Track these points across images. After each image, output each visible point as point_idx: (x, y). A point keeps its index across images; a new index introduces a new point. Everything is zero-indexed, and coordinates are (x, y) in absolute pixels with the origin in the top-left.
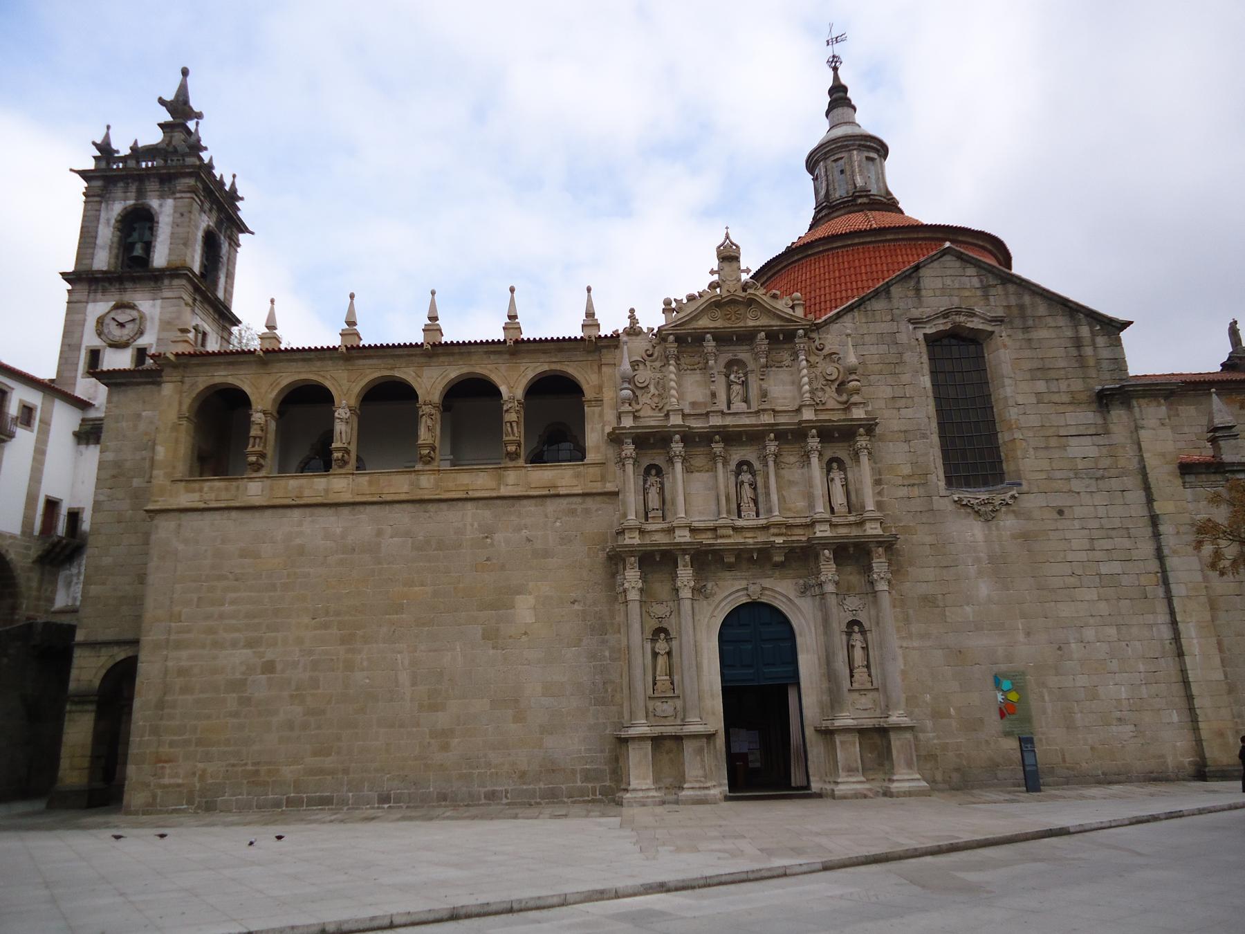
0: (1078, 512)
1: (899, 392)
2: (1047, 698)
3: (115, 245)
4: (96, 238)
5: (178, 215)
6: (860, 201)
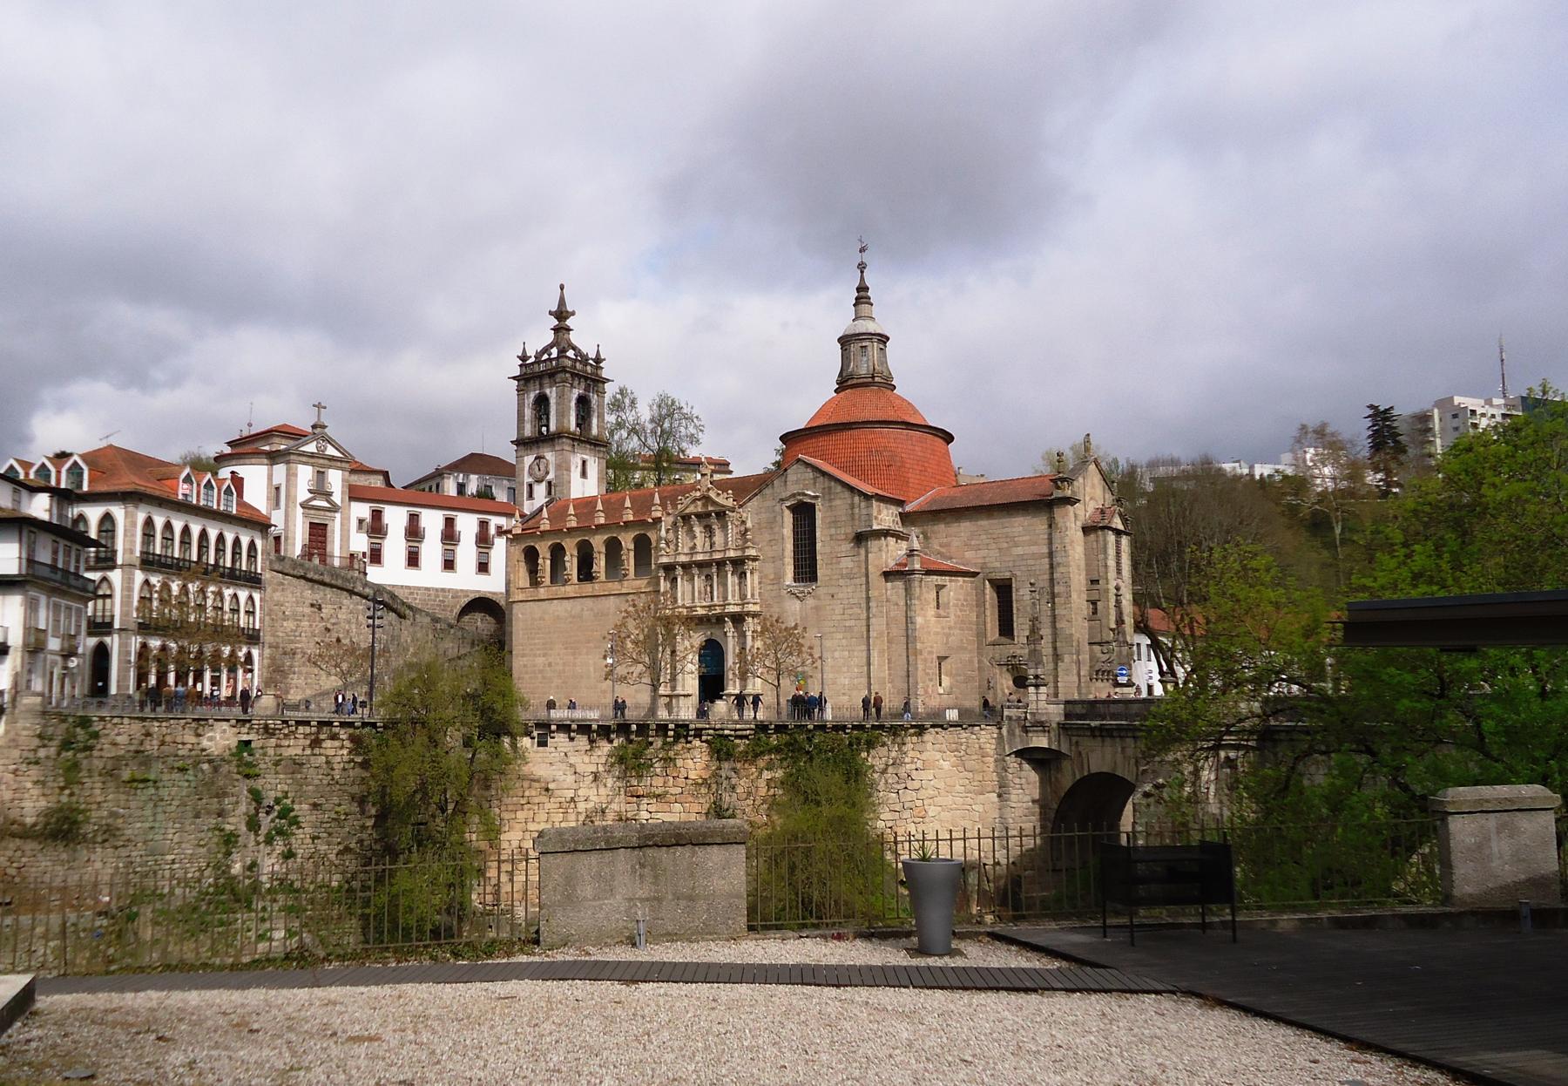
0: (840, 596)
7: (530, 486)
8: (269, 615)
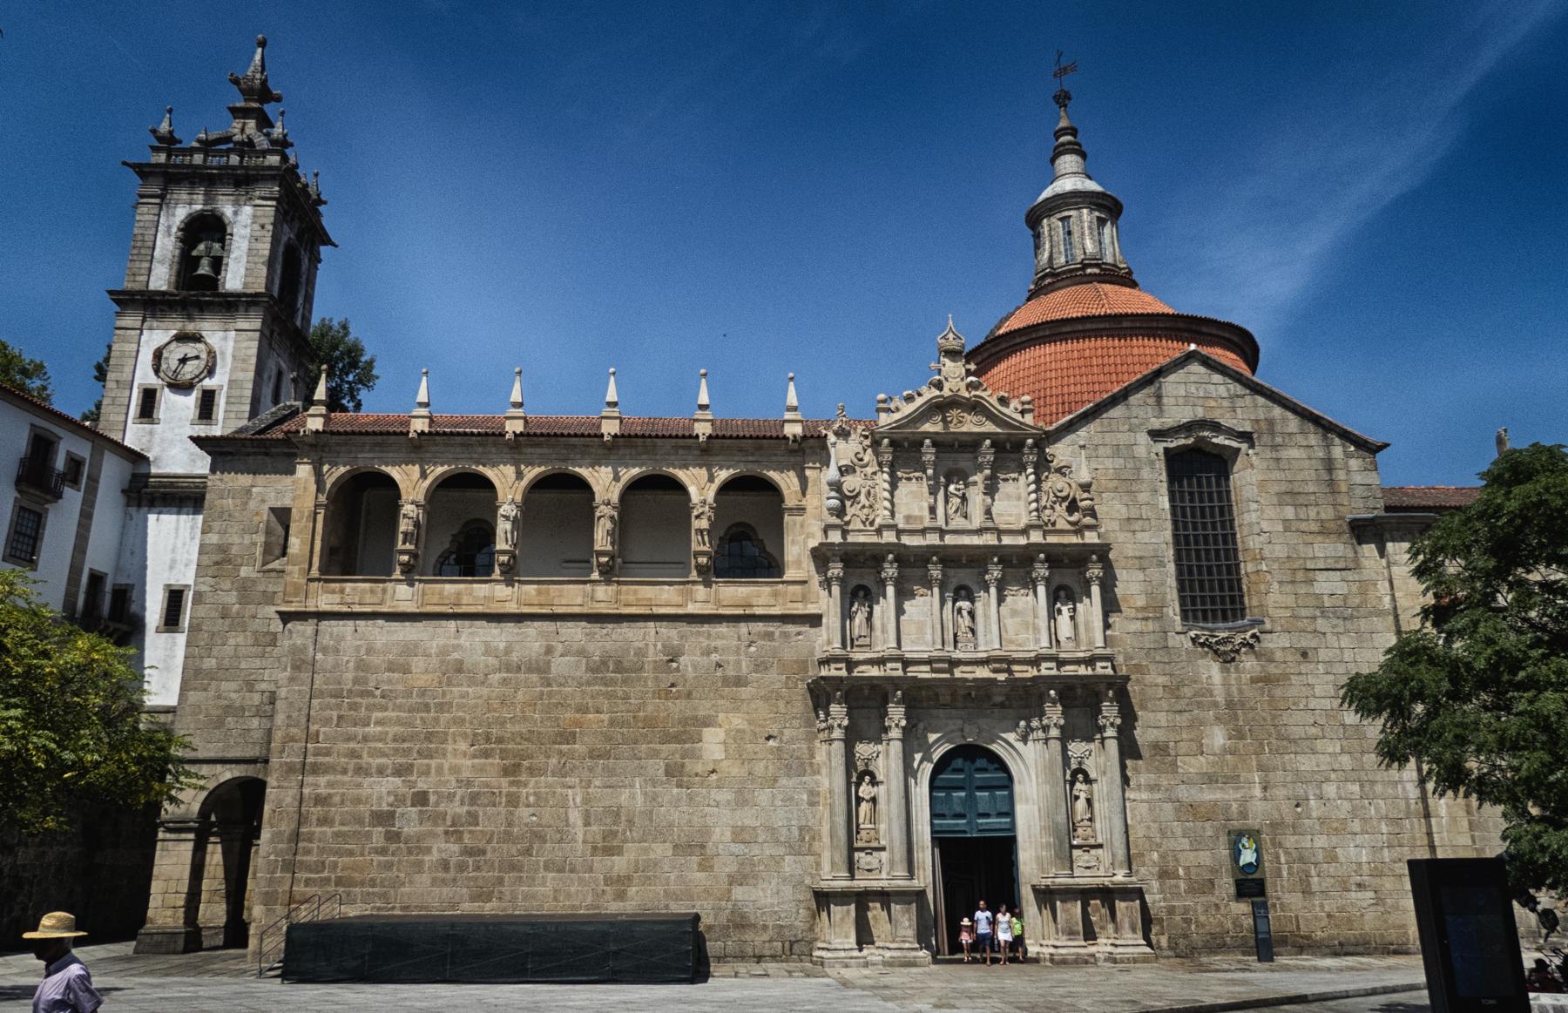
0: (1323, 654)
1: (1134, 513)
2: (1283, 860)
3: (176, 259)
4: (154, 248)
5: (257, 227)
6: (1089, 271)
7: (149, 397)
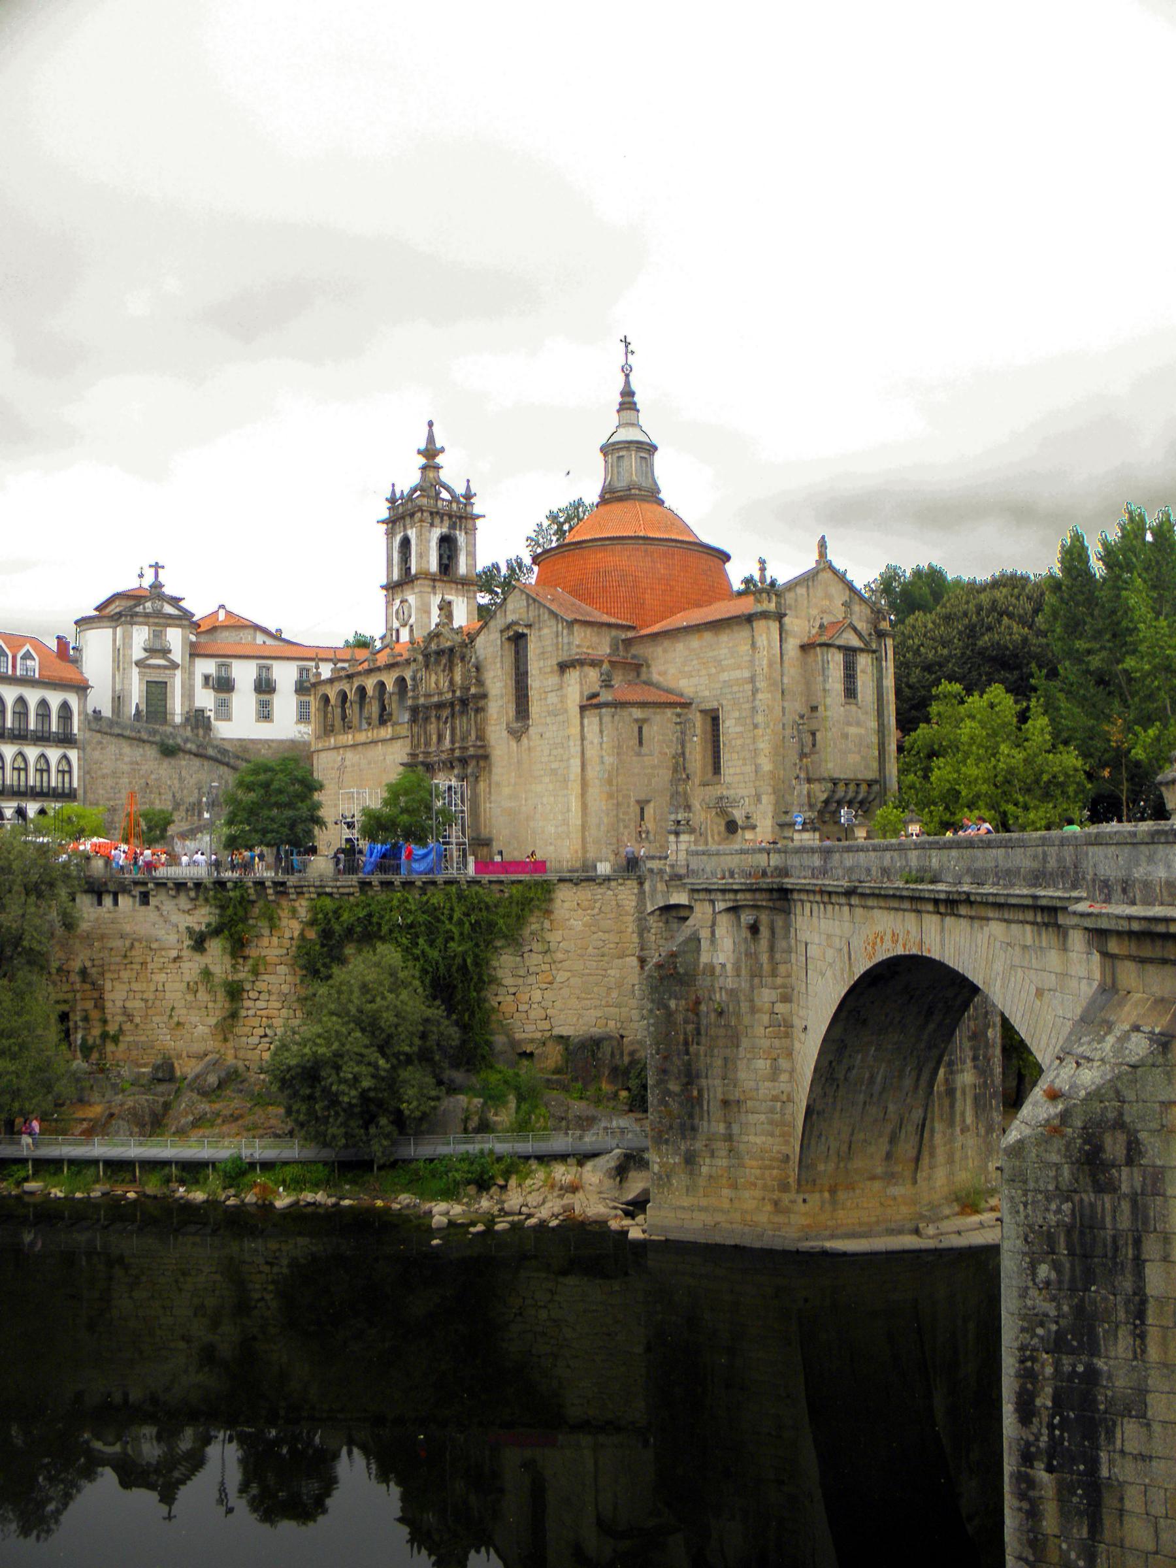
0: (547, 735)
7: (398, 631)
8: (88, 772)
